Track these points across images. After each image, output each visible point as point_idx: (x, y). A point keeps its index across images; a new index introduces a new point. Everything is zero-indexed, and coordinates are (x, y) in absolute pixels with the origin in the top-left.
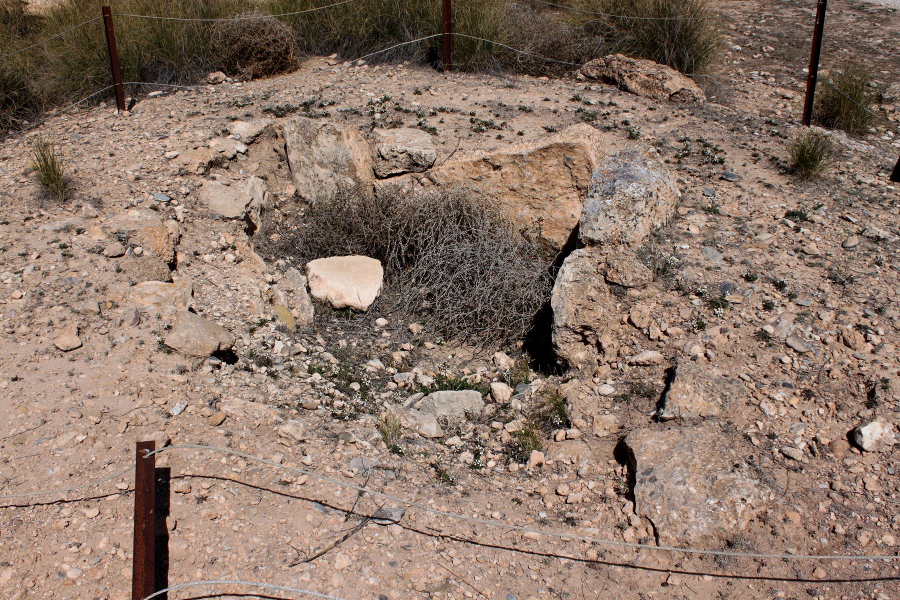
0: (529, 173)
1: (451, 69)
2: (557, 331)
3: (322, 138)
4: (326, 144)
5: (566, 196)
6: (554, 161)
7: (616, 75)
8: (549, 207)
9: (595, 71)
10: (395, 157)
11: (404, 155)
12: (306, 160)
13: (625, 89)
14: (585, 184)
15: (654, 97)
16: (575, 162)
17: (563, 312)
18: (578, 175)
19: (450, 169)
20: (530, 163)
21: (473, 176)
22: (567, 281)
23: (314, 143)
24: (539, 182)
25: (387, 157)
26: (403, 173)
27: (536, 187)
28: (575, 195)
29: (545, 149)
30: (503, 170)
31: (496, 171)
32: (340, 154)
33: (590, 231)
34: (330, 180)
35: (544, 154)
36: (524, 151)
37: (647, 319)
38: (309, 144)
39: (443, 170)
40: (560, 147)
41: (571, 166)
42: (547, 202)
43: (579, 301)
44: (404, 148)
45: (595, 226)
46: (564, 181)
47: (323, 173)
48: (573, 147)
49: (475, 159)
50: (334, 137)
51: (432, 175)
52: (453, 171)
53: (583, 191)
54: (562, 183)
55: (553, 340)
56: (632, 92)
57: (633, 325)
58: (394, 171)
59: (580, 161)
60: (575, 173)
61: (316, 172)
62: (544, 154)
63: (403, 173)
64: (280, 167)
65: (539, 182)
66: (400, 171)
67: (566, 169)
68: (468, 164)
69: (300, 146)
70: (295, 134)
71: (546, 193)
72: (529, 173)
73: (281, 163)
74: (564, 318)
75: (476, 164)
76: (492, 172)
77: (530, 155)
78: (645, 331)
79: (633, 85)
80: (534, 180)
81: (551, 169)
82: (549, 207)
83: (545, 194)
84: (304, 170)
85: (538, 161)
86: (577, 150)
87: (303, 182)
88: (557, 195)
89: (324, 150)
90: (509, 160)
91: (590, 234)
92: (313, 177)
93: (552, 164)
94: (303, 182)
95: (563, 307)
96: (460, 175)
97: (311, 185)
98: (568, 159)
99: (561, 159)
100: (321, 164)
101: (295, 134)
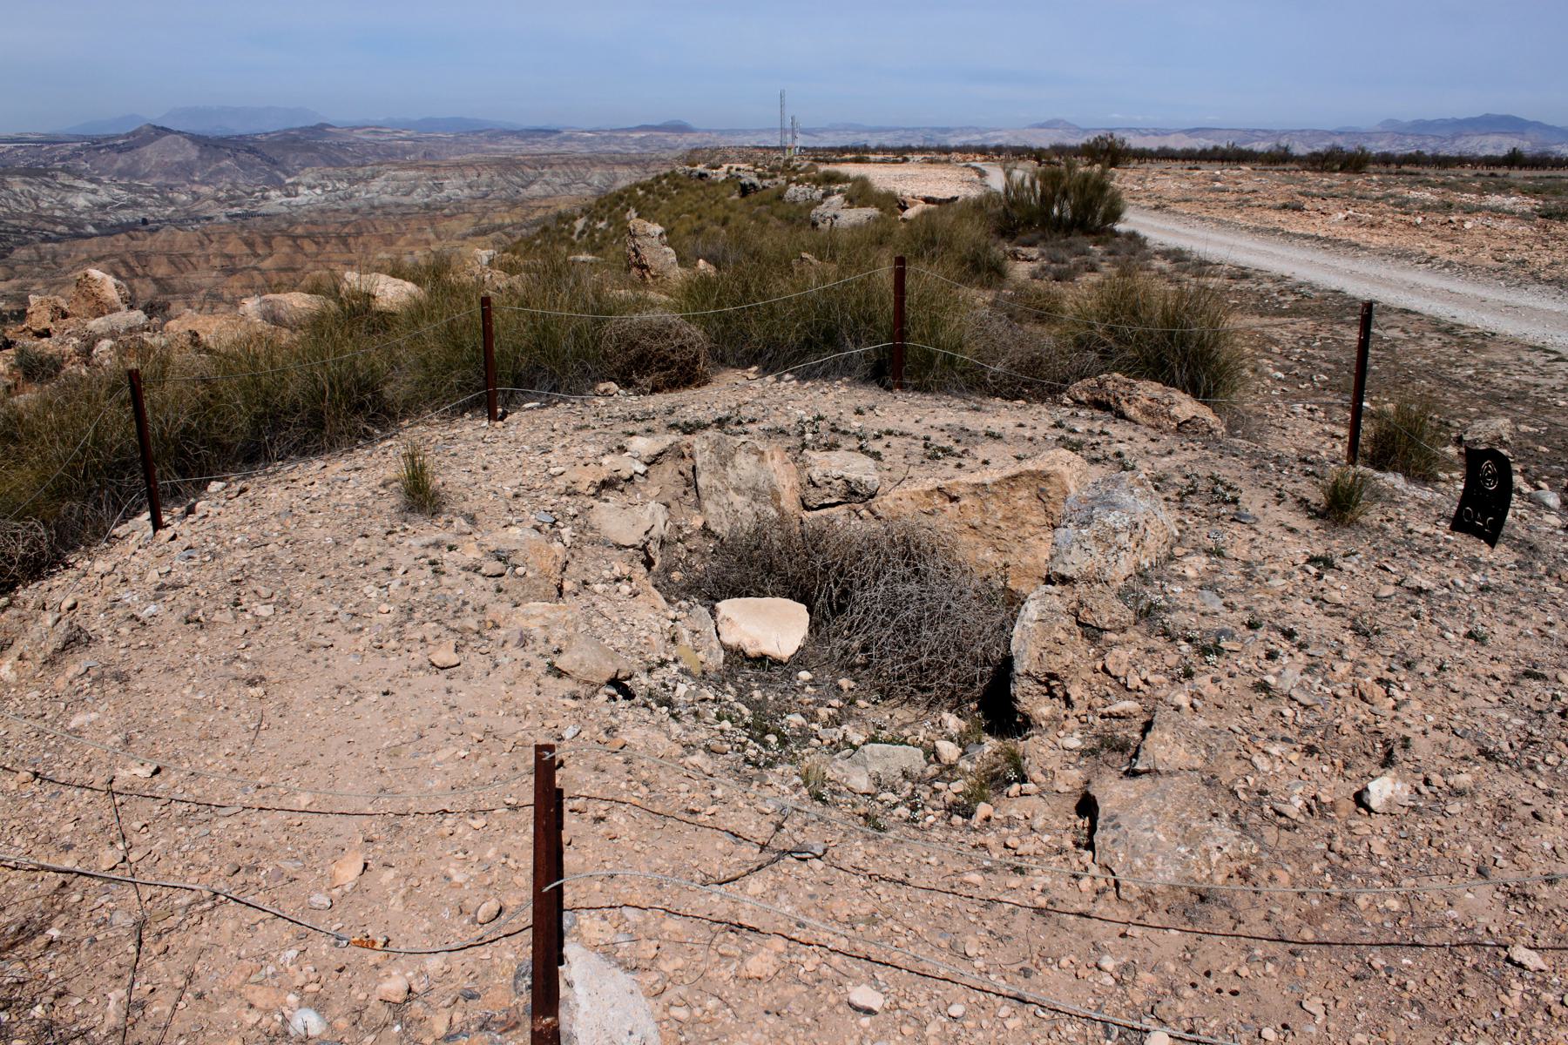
1: (902, 387)
3: (740, 459)
6: (1025, 493)
8: (1018, 549)
13: (1121, 415)
15: (1159, 427)
20: (995, 494)
24: (1005, 518)
27: (1002, 525)
29: (1014, 478)
34: (748, 510)
36: (987, 480)
37: (1125, 666)
38: (724, 465)
39: (888, 501)
44: (840, 473)
45: (1068, 559)
46: (1038, 518)
47: (739, 501)
49: (927, 488)
50: (755, 458)
51: (874, 506)
54: (1034, 520)
56: (1130, 420)
58: (827, 501)
64: (686, 493)
65: (1005, 518)
66: (834, 500)
75: (929, 494)
76: (948, 504)
77: (995, 484)
79: (1131, 411)
80: (999, 515)
82: (1018, 549)
83: (1012, 533)
84: (715, 497)
90: (969, 490)
96: (908, 508)
98: (1042, 490)
99: (1033, 490)
100: (737, 490)
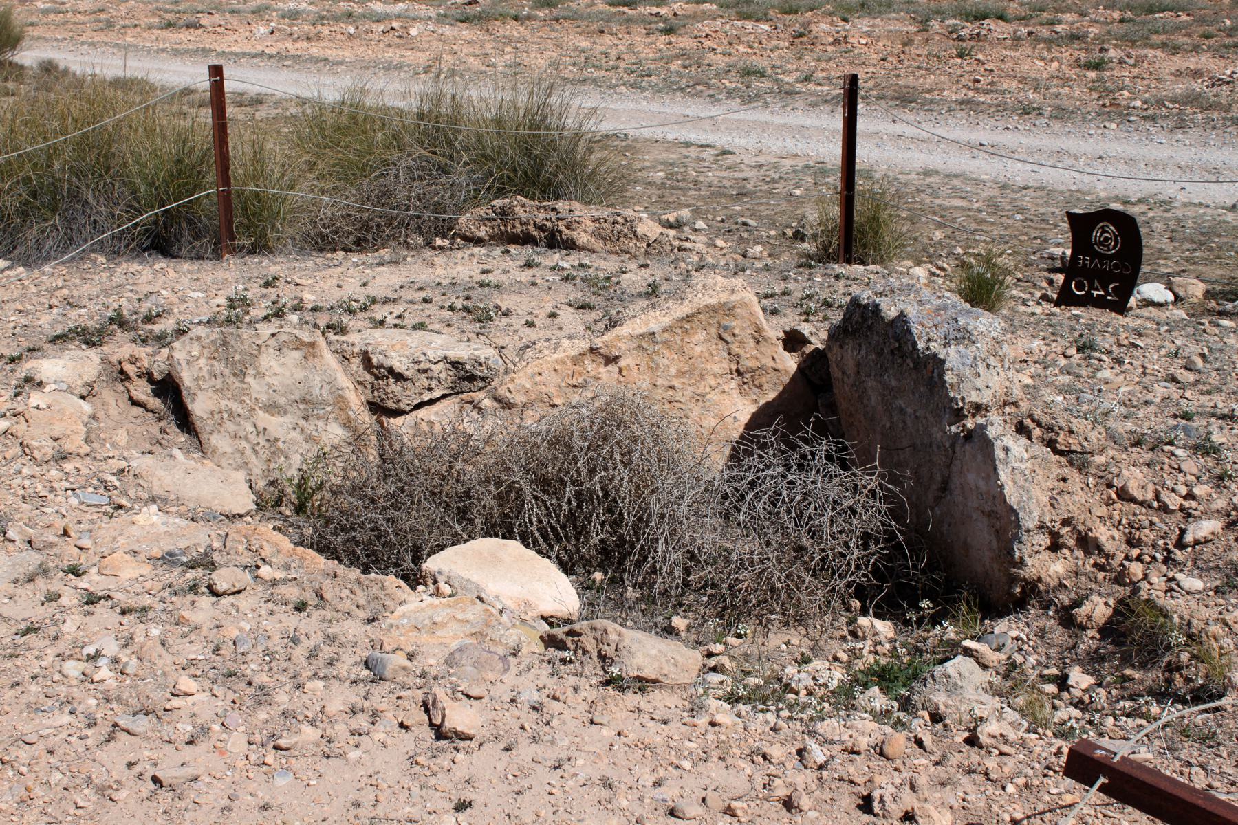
0: (665, 361)
1: (233, 250)
2: (1024, 538)
3: (268, 361)
4: (278, 370)
5: (720, 388)
6: (701, 336)
7: (531, 229)
8: (696, 411)
9: (483, 228)
10: (425, 371)
11: (441, 365)
12: (235, 406)
13: (571, 245)
14: (751, 364)
15: (624, 252)
16: (736, 331)
17: (1033, 505)
18: (741, 352)
19: (533, 375)
20: (666, 344)
21: (574, 382)
22: (1022, 460)
23: (251, 371)
24: (681, 373)
25: (408, 374)
26: (444, 396)
27: (676, 383)
28: (733, 384)
29: (689, 318)
30: (622, 363)
31: (610, 367)
32: (317, 382)
33: (973, 393)
34: (293, 434)
35: (687, 326)
36: (655, 327)
37: (1151, 487)
38: (241, 375)
39: (522, 379)
40: (712, 309)
41: (729, 339)
42: (692, 405)
43: (1049, 484)
44: (441, 353)
45: (979, 383)
46: (720, 365)
47: (276, 425)
48: (734, 307)
49: (574, 352)
50: (297, 355)
51: (502, 391)
52: (538, 378)
53: (748, 376)
54: (716, 368)
55: (1017, 554)
56: (584, 249)
57: (1132, 500)
58: (426, 397)
59: (743, 329)
60: (735, 349)
61: (261, 426)
62: (687, 326)
63: (444, 396)
64: (163, 431)
65: (681, 373)
66: (437, 394)
67: (721, 344)
68: (564, 363)
69: (219, 383)
70: (202, 361)
71: (691, 389)
72: (665, 361)
73: (162, 424)
74: (1036, 514)
75: (577, 360)
76: (602, 369)
77: (665, 330)
78: (1155, 504)
79: (583, 238)
80: (673, 371)
81: (698, 349)
82: (696, 411)
83: (689, 391)
84: (230, 427)
85: (678, 338)
86: (738, 311)
87: (229, 450)
88: (708, 389)
89: (275, 381)
90: (632, 345)
91: (974, 398)
92: (252, 437)
93: (700, 341)
94: (229, 450)
95: (1029, 499)
96: (551, 384)
97: (249, 452)
98: (726, 328)
99: (713, 330)
100: (272, 408)
101: (202, 361)
